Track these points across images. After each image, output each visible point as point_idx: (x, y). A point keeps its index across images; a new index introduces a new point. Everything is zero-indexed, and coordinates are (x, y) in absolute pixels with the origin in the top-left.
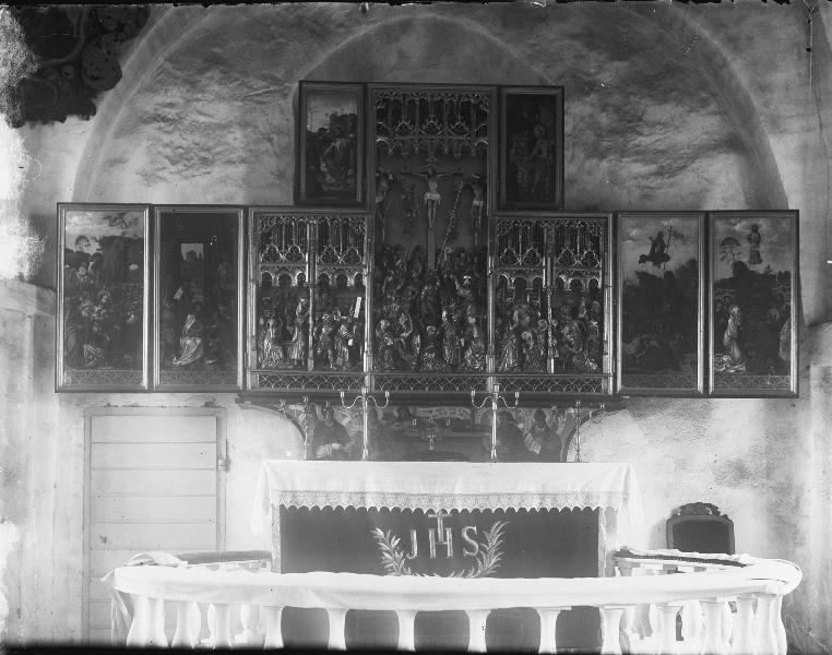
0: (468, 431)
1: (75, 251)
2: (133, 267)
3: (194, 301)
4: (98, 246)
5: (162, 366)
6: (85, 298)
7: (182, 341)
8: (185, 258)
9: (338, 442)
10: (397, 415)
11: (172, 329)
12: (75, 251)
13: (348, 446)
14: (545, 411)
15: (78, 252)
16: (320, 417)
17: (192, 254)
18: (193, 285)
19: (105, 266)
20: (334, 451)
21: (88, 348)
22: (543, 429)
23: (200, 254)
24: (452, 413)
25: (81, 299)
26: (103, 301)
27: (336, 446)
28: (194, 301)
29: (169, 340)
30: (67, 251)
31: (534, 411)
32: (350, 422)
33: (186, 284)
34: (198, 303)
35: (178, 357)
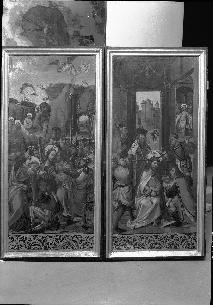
1: (20, 101)
2: (83, 119)
3: (150, 156)
4: (46, 96)
5: (117, 229)
6: (31, 154)
7: (137, 201)
8: (140, 109)
11: (126, 188)
12: (20, 101)
15: (23, 103)
17: (147, 103)
18: (149, 136)
19: (52, 118)
21: (34, 210)
23: (157, 103)
25: (26, 155)
26: (51, 156)
28: (150, 156)
29: (125, 202)
30: (11, 101)
33: (141, 137)
34: (154, 158)
35: (133, 218)
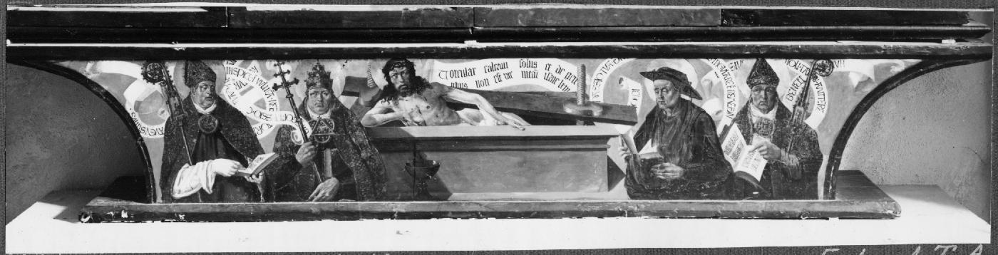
0: (570, 120)
9: (231, 154)
10: (380, 80)
13: (257, 163)
14: (777, 65)
16: (183, 91)
20: (219, 178)
22: (771, 115)
24: (525, 75)
27: (226, 166)
31: (750, 63)
32: (261, 104)
